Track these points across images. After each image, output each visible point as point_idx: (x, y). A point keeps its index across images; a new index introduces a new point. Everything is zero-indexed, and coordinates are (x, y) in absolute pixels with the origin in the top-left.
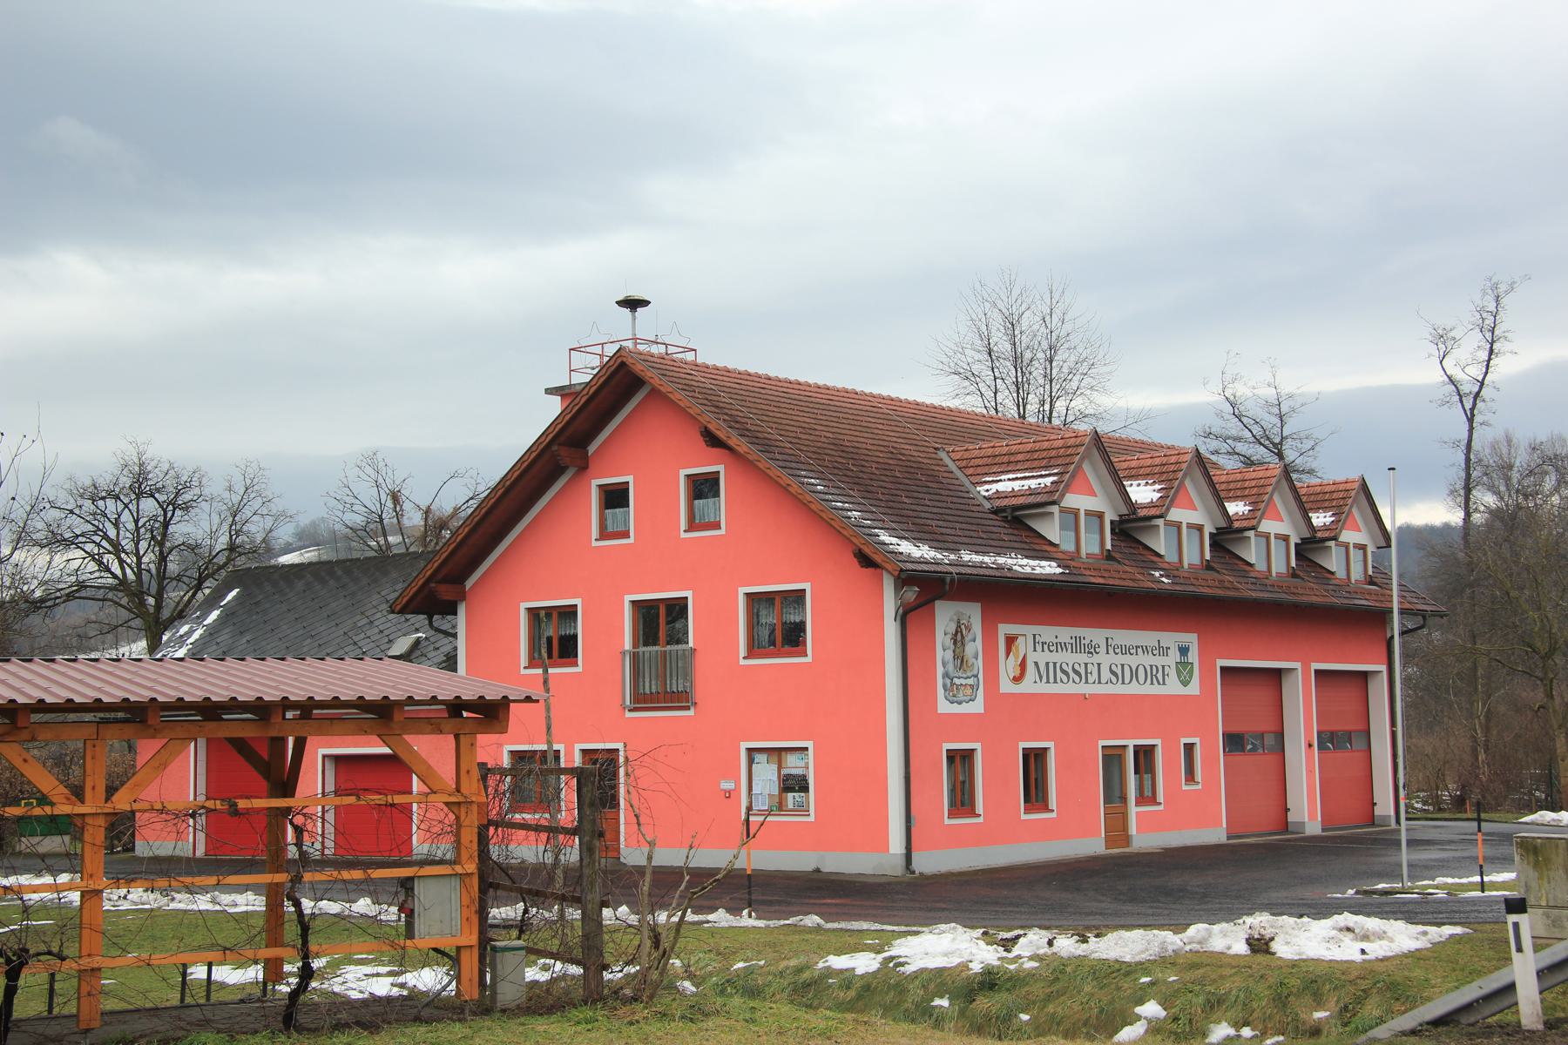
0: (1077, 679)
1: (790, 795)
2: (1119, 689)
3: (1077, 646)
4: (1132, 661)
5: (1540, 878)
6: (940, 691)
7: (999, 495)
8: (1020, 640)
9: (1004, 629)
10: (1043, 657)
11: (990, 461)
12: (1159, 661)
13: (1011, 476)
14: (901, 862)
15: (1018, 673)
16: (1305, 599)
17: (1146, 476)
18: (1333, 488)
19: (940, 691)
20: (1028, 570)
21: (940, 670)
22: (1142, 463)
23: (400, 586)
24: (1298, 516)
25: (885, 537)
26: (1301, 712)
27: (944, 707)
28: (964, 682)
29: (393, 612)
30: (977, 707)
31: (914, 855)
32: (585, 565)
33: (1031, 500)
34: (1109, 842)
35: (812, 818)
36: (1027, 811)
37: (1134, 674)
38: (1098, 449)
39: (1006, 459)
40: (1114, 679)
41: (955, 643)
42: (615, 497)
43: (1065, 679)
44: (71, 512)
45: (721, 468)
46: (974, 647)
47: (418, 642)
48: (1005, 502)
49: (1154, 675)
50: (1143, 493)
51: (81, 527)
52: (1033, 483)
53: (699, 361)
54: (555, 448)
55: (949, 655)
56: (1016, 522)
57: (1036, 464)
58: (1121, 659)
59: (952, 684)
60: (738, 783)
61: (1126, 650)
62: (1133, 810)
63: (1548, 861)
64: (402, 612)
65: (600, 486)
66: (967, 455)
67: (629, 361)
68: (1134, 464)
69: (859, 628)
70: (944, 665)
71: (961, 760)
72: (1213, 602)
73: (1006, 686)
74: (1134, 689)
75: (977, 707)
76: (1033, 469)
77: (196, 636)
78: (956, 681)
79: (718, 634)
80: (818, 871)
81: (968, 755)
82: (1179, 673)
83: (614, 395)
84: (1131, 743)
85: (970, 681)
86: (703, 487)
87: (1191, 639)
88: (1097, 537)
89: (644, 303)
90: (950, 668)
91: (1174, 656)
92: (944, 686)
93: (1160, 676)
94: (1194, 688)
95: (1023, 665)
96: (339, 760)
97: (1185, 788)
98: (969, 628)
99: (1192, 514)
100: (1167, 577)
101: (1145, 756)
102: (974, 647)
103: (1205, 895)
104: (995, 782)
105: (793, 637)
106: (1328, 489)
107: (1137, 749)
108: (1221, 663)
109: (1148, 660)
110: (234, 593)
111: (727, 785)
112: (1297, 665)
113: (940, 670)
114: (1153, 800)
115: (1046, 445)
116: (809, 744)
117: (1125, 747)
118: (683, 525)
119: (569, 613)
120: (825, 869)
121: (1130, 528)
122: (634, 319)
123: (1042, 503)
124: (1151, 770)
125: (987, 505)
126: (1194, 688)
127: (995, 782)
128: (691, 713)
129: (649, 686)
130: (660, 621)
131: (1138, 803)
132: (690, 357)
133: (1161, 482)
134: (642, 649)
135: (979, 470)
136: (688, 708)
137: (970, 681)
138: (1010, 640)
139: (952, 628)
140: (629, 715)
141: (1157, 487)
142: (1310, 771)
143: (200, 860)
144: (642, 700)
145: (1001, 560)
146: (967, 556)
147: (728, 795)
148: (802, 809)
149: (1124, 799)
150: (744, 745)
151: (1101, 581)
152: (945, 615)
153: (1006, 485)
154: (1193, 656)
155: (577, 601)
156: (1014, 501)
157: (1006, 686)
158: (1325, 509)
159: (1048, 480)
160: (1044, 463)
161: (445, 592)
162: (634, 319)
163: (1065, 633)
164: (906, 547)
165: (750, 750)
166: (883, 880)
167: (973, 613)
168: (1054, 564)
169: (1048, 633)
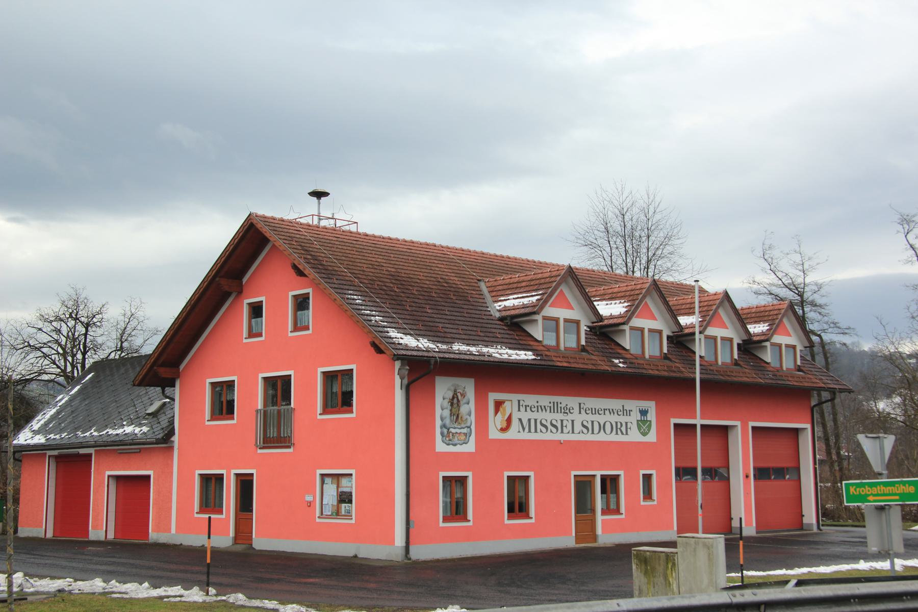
0: (554, 430)
1: (343, 505)
2: (589, 437)
3: (555, 408)
4: (602, 419)
5: (648, 583)
6: (438, 437)
7: (506, 309)
8: (507, 405)
9: (493, 397)
10: (525, 416)
11: (505, 287)
12: (623, 419)
13: (515, 296)
14: (402, 552)
15: (504, 425)
16: (735, 379)
17: (621, 297)
18: (771, 308)
19: (438, 437)
20: (506, 356)
21: (438, 423)
22: (621, 289)
23: (138, 369)
24: (668, 316)
25: (393, 333)
26: (741, 457)
27: (441, 447)
28: (458, 431)
29: (134, 385)
30: (470, 447)
31: (411, 548)
32: (240, 356)
33: (522, 311)
34: (578, 540)
35: (353, 521)
36: (509, 518)
37: (602, 428)
38: (573, 278)
39: (515, 285)
40: (585, 431)
41: (452, 404)
42: (256, 310)
43: (544, 430)
44: (40, 329)
45: (309, 290)
46: (469, 408)
47: (164, 404)
48: (508, 313)
49: (617, 428)
50: (610, 309)
51: (44, 338)
52: (526, 301)
53: (360, 231)
54: (217, 279)
55: (447, 413)
56: (514, 327)
57: (531, 288)
58: (590, 417)
59: (449, 432)
60: (315, 497)
61: (596, 412)
62: (599, 518)
63: (653, 569)
64: (140, 385)
65: (249, 304)
66: (496, 284)
67: (255, 222)
68: (616, 290)
69: (384, 395)
70: (442, 419)
71: (456, 484)
72: (660, 382)
73: (494, 434)
74: (602, 437)
75: (470, 447)
76: (525, 292)
77: (63, 401)
78: (452, 430)
79: (308, 396)
80: (356, 556)
81: (462, 481)
82: (639, 427)
83: (251, 244)
84: (599, 474)
85: (465, 431)
86: (301, 303)
87: (650, 406)
88: (574, 337)
89: (325, 194)
90: (447, 422)
91: (636, 416)
92: (442, 434)
93: (623, 429)
94: (652, 437)
95: (509, 420)
96: (118, 478)
97: (642, 503)
98: (463, 395)
99: (653, 322)
100: (623, 363)
101: (610, 484)
102: (469, 408)
103: (576, 582)
104: (485, 498)
105: (346, 401)
106: (768, 309)
107: (604, 479)
108: (674, 421)
109: (614, 418)
110: (90, 376)
111: (309, 498)
112: (738, 423)
113: (438, 423)
114: (617, 511)
115: (540, 276)
116: (353, 471)
117: (594, 476)
118: (290, 327)
119: (230, 384)
120: (360, 556)
121: (604, 333)
122: (319, 203)
123: (530, 313)
124: (616, 491)
125: (498, 315)
126: (652, 437)
127: (485, 498)
128: (291, 450)
129: (272, 433)
130: (279, 389)
131: (604, 512)
132: (353, 228)
133: (628, 301)
134: (271, 408)
135: (499, 293)
136: (289, 447)
137: (465, 431)
138: (498, 404)
139: (450, 394)
140: (260, 451)
141: (626, 304)
142: (747, 494)
143: (49, 540)
144: (268, 442)
145: (485, 350)
146: (456, 347)
147: (310, 504)
148: (348, 515)
149: (593, 511)
150: (320, 471)
151: (565, 364)
152: (443, 388)
153: (512, 302)
154: (652, 416)
155: (235, 378)
156: (513, 312)
157: (494, 434)
158: (764, 321)
159: (534, 299)
160: (536, 287)
161: (164, 372)
162: (319, 203)
163: (545, 400)
164: (410, 341)
165: (323, 475)
166: (381, 564)
167: (468, 386)
168: (530, 353)
169: (530, 399)
